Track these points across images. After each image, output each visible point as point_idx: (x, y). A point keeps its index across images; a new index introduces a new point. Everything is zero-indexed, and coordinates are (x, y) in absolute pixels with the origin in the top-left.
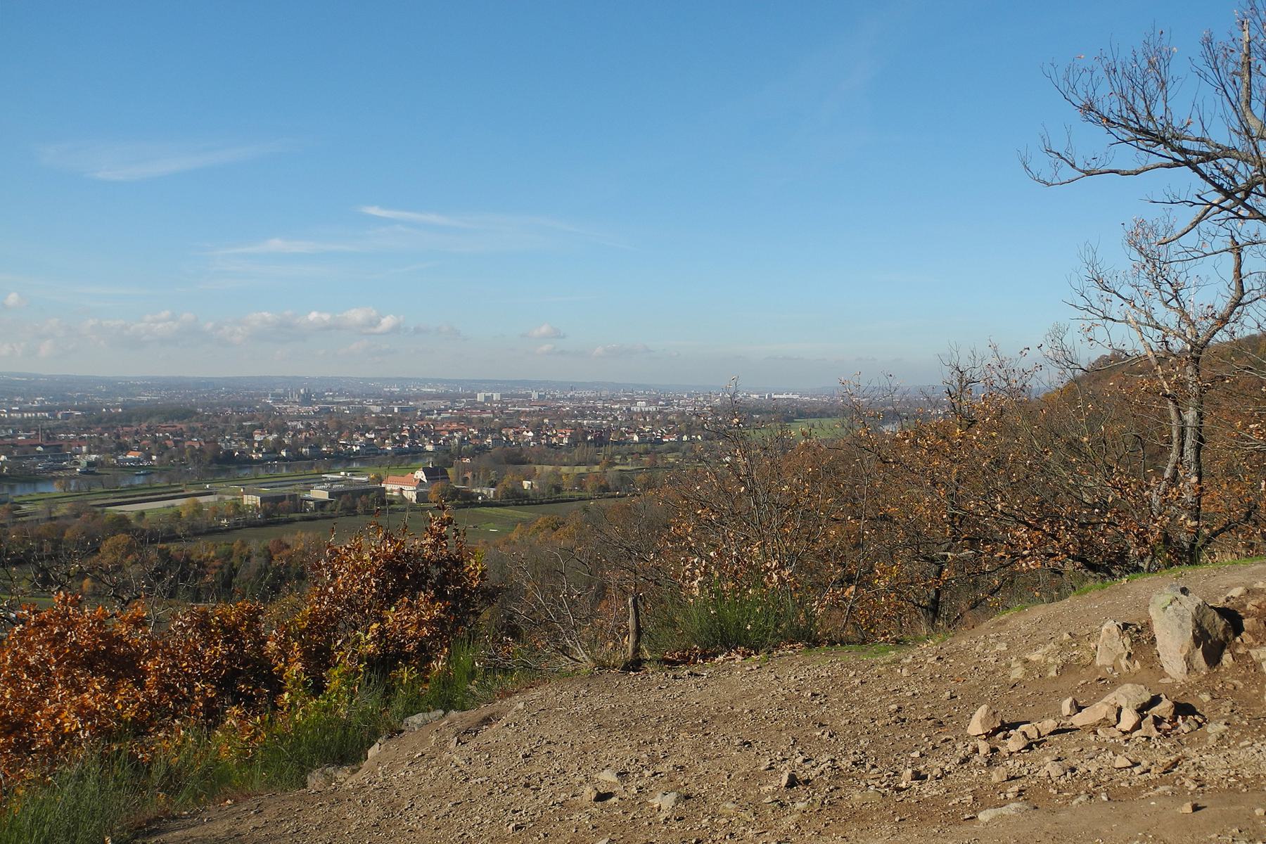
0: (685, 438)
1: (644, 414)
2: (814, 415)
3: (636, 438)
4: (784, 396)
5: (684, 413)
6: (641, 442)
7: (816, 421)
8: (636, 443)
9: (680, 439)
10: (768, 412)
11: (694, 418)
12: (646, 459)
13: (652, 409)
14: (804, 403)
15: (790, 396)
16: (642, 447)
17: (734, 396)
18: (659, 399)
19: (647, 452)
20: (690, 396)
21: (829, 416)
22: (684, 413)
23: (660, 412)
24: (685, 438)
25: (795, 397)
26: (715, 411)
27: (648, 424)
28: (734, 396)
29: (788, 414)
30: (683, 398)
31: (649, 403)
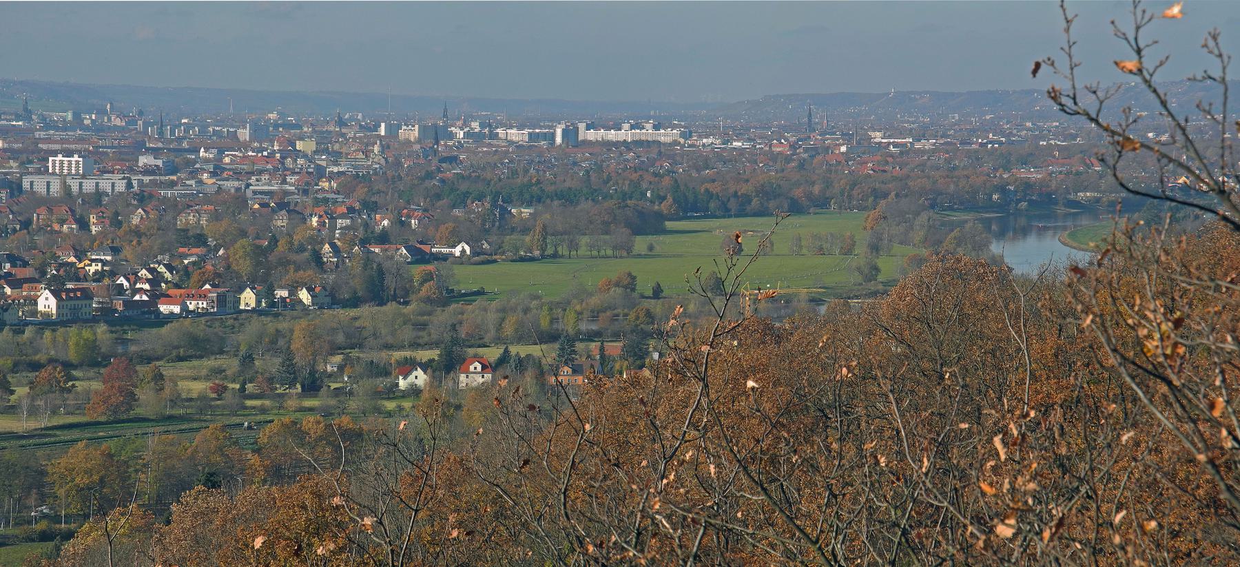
0: (248, 298)
1: (76, 206)
2: (742, 207)
3: (47, 302)
4: (625, 134)
5: (240, 201)
6: (69, 317)
7: (752, 230)
8: (47, 323)
9: (227, 303)
10: (568, 198)
11: (281, 221)
12: (89, 384)
13: (114, 184)
14: (702, 161)
15: (648, 132)
16: (72, 341)
17: (436, 133)
18: (139, 147)
19: (94, 359)
20: (260, 132)
21: (796, 209)
22: (240, 201)
23: (143, 198)
24: (248, 298)
25: (667, 136)
26: (366, 193)
27: (96, 243)
28: (436, 133)
29: (649, 201)
30: (233, 142)
31: (97, 162)
